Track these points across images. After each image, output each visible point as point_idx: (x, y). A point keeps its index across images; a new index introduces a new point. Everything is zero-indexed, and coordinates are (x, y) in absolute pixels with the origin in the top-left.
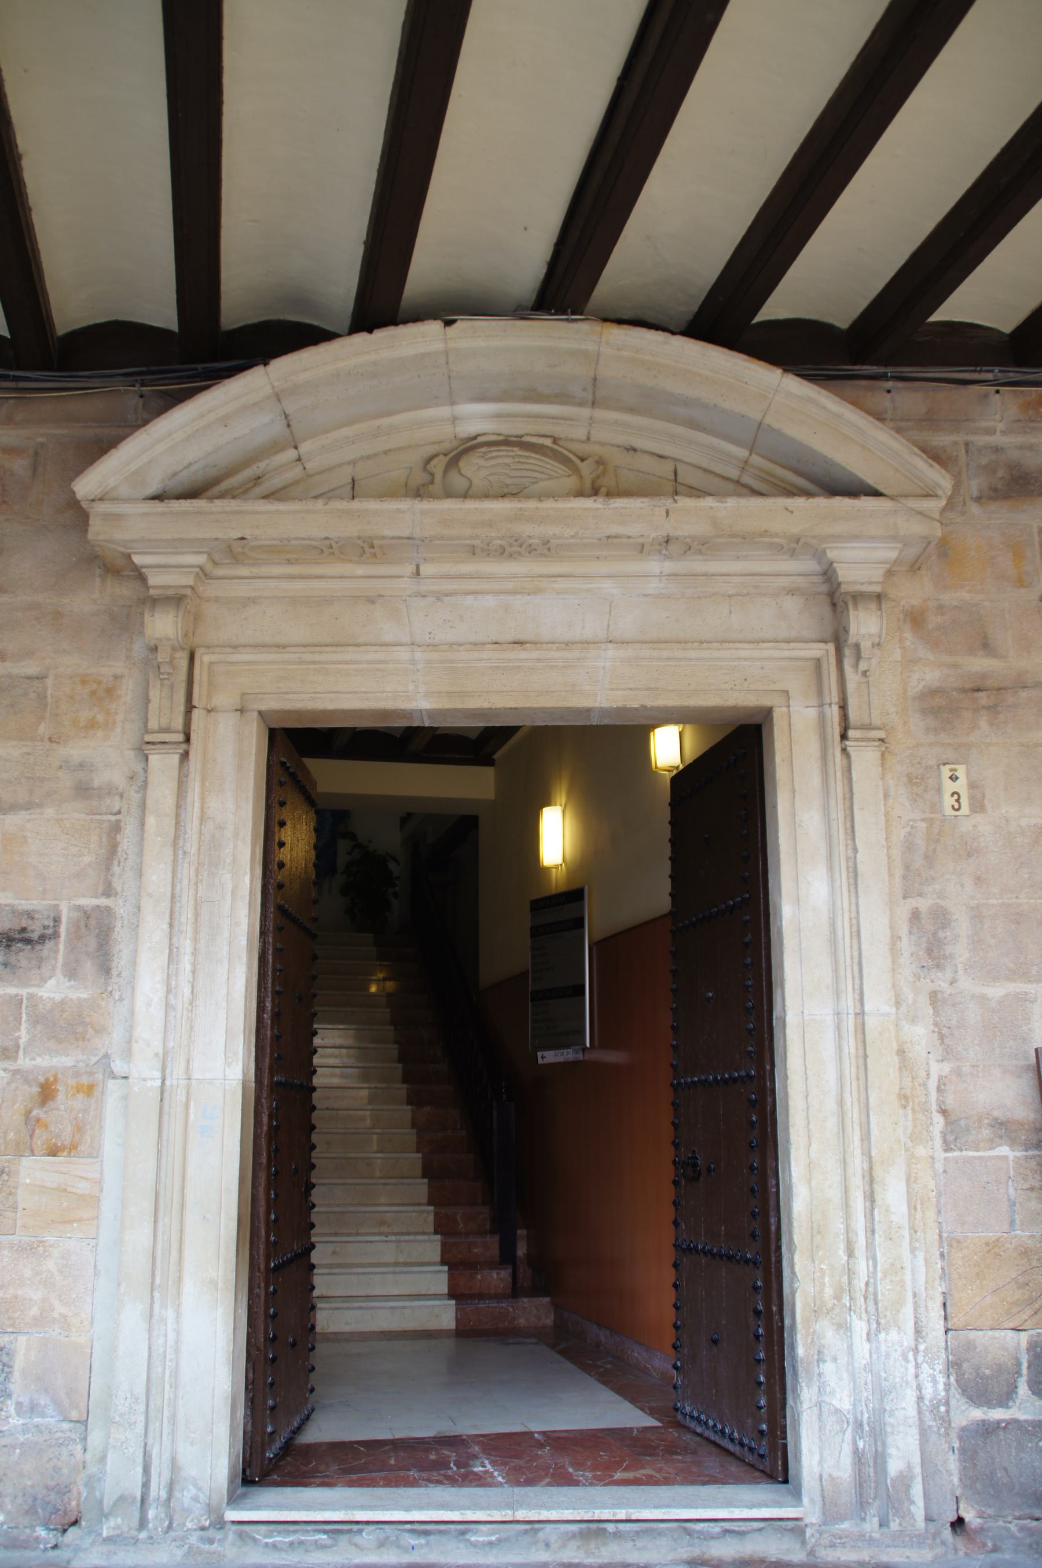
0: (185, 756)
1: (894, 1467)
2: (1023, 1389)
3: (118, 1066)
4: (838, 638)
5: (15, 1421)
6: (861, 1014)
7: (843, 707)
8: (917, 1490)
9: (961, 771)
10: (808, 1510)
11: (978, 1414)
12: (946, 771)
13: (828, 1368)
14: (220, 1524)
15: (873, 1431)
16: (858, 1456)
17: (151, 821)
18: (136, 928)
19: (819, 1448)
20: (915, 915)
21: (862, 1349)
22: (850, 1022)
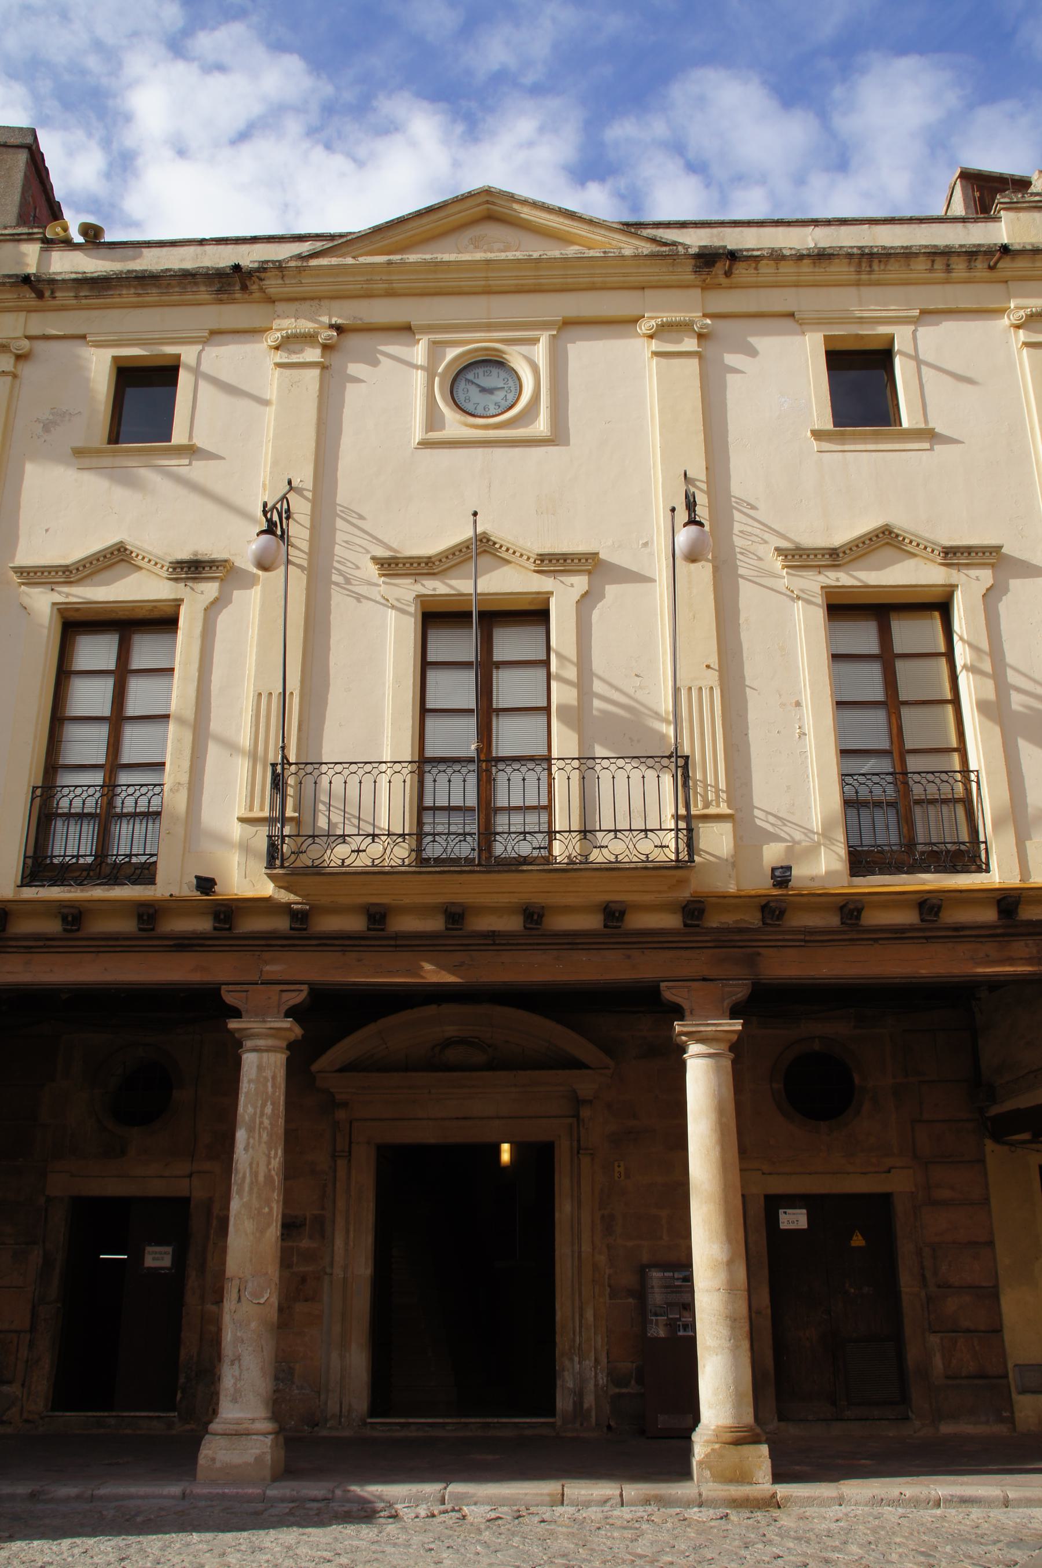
0: (349, 1161)
1: (586, 1406)
2: (633, 1382)
3: (328, 1270)
4: (577, 1116)
5: (296, 1391)
6: (580, 1252)
7: (579, 1141)
8: (593, 1414)
9: (622, 1164)
10: (558, 1420)
11: (617, 1390)
12: (616, 1164)
13: (566, 1373)
14: (365, 1424)
15: (579, 1394)
16: (574, 1402)
17: (338, 1184)
18: (334, 1222)
19: (563, 1403)
20: (603, 1217)
21: (577, 1366)
22: (576, 1255)
